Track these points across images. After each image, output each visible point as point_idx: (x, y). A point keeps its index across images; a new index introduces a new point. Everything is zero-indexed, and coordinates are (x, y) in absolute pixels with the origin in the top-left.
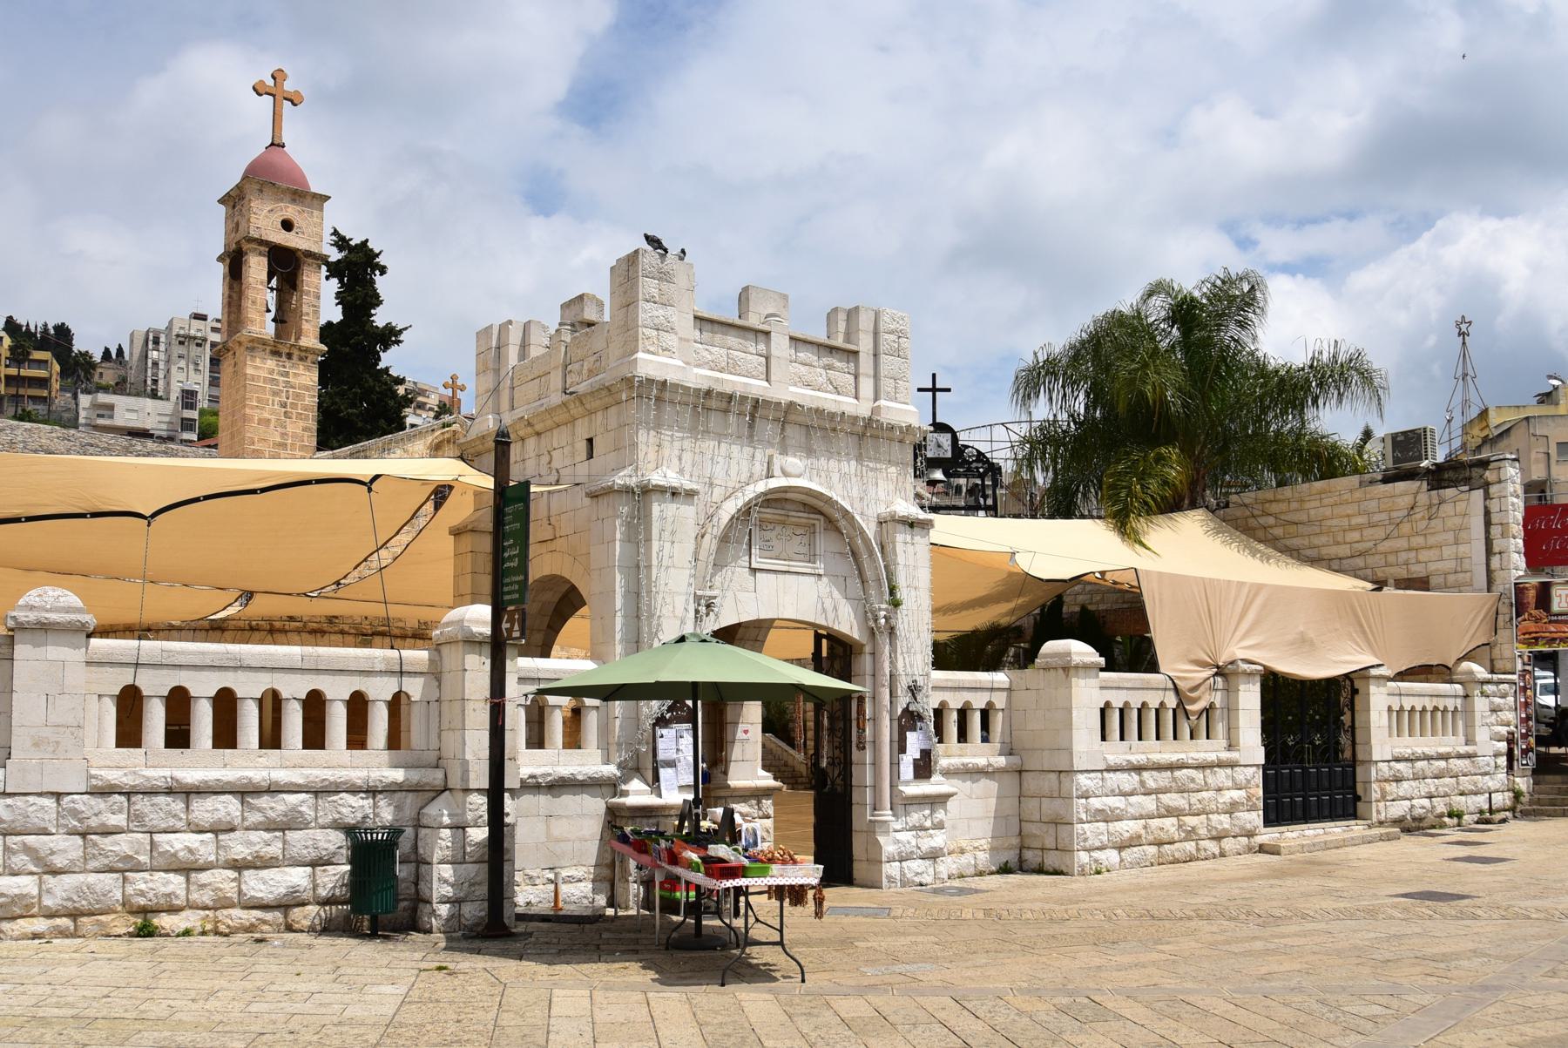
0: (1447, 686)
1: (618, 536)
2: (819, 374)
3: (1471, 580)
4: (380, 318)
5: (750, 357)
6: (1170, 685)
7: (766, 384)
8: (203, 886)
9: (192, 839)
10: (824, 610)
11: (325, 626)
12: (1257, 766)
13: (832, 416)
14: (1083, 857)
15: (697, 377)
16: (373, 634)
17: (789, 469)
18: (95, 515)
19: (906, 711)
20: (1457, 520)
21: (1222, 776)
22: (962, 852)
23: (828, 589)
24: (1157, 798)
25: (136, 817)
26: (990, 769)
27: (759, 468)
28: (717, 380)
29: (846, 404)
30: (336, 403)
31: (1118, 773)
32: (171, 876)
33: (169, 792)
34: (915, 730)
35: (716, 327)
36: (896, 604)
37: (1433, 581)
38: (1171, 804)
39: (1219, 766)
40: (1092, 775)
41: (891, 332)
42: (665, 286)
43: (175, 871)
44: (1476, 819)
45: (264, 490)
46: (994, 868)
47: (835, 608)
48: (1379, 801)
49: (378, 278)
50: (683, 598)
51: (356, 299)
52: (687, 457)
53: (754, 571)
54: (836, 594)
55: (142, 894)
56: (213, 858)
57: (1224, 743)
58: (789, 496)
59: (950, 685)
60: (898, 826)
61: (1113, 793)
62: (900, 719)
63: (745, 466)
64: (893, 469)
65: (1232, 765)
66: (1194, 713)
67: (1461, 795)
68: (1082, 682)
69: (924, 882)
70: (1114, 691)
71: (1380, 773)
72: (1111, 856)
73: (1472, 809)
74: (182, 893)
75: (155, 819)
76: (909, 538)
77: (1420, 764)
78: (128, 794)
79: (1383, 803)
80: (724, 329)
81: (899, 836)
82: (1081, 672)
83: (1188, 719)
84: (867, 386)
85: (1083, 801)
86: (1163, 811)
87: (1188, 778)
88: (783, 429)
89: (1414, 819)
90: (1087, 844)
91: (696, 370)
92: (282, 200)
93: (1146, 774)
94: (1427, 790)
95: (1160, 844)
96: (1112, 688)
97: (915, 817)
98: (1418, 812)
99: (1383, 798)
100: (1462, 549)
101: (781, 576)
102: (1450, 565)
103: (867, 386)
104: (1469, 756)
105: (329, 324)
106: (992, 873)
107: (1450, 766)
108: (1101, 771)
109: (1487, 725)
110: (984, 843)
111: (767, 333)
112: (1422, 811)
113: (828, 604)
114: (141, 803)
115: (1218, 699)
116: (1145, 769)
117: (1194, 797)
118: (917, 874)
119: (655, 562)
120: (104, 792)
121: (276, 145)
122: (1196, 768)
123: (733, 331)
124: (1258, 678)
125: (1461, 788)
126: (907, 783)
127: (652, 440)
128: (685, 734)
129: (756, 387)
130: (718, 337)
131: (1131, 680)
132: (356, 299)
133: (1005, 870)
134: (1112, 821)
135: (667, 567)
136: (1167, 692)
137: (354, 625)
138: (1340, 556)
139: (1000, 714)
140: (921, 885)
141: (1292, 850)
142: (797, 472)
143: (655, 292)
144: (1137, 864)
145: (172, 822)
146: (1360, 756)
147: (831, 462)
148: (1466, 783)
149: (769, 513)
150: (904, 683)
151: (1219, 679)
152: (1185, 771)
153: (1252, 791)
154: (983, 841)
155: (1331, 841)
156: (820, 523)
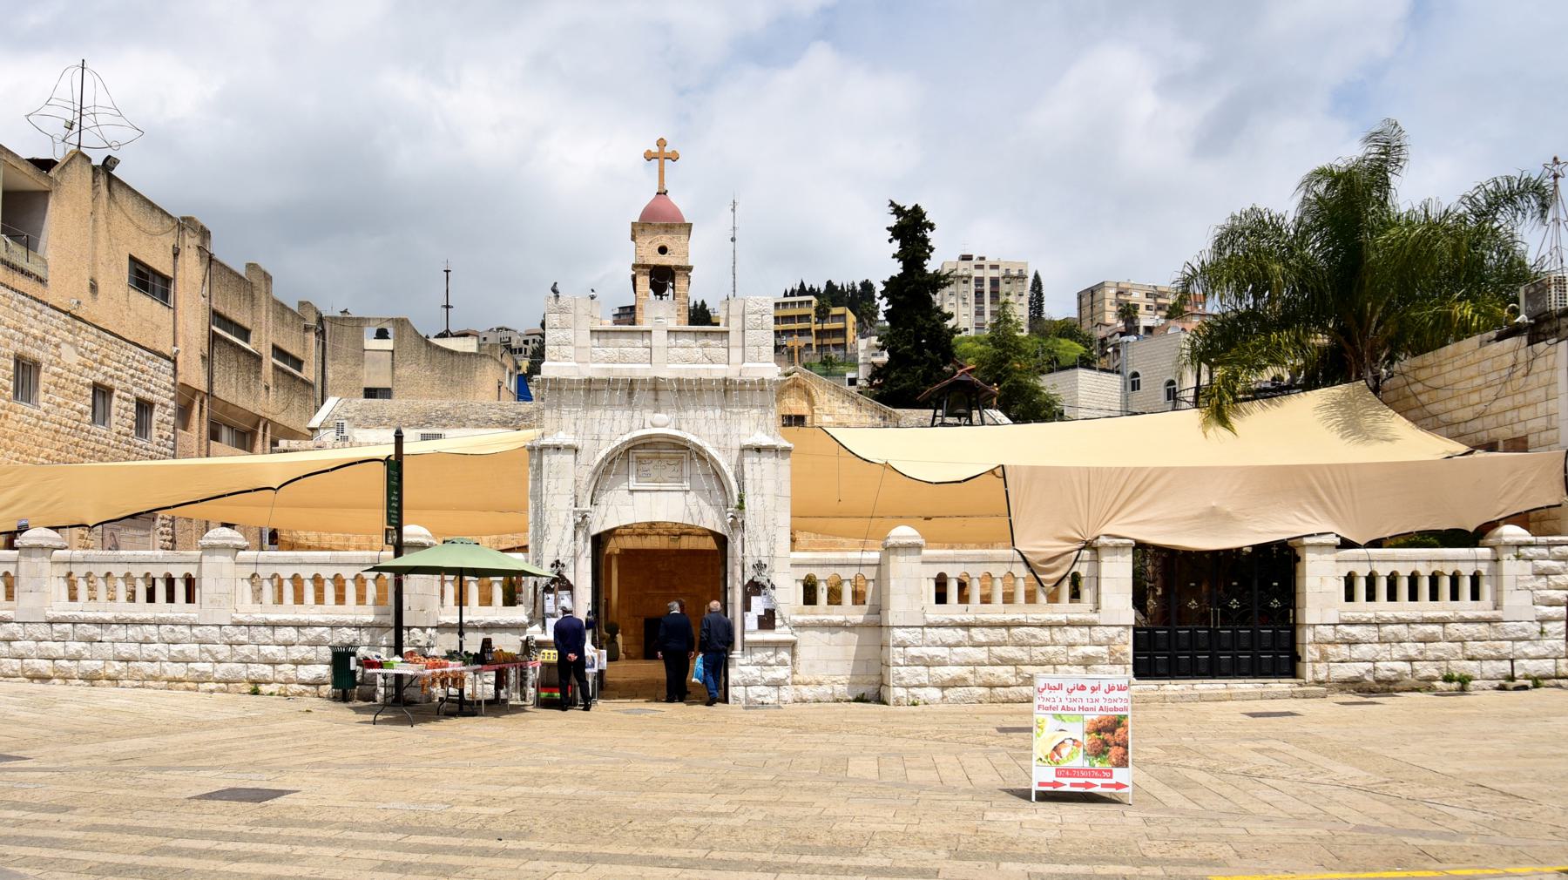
0: (1465, 550)
1: (530, 477)
2: (697, 352)
3: (1558, 437)
4: (931, 266)
5: (637, 350)
6: (1019, 558)
7: (649, 366)
8: (280, 672)
9: (274, 649)
10: (691, 514)
11: (647, 531)
12: (1127, 626)
13: (689, 382)
14: (899, 692)
15: (594, 370)
16: (681, 534)
17: (655, 422)
18: (256, 490)
19: (751, 582)
20: (1547, 375)
21: (1074, 634)
22: (820, 684)
23: (695, 500)
24: (989, 650)
25: (252, 637)
26: (848, 624)
27: (636, 423)
28: (608, 369)
29: (719, 371)
30: (893, 343)
31: (940, 629)
32: (266, 666)
33: (265, 625)
34: (759, 595)
35: (610, 335)
36: (741, 507)
37: (1532, 440)
38: (1003, 654)
39: (1068, 625)
40: (910, 629)
41: (755, 313)
42: (564, 317)
43: (269, 664)
44: (1497, 685)
45: (333, 469)
46: (850, 698)
47: (701, 512)
48: (1317, 662)
49: (929, 234)
50: (565, 513)
51: (907, 256)
52: (580, 423)
53: (632, 491)
54: (702, 502)
55: (253, 674)
56: (284, 658)
57: (1091, 606)
58: (653, 440)
59: (816, 562)
60: (744, 662)
61: (934, 644)
62: (747, 585)
63: (625, 423)
64: (755, 411)
65: (1090, 625)
66: (1048, 581)
67: (1469, 659)
68: (901, 559)
69: (765, 702)
70: (949, 565)
71: (1317, 635)
72: (935, 693)
73: (1491, 674)
74: (271, 675)
75: (260, 638)
76: (756, 460)
77: (1387, 629)
78: (248, 626)
79: (1324, 664)
80: (617, 334)
81: (743, 669)
82: (900, 551)
83: (1042, 585)
84: (736, 354)
85: (901, 649)
86: (994, 660)
87: (1027, 634)
88: (657, 394)
89: (1378, 681)
90: (903, 682)
91: (592, 366)
92: (657, 233)
93: (973, 631)
94: (1402, 653)
95: (991, 686)
96: (946, 562)
97: (759, 656)
98: (1381, 674)
99: (1324, 657)
100: (1551, 404)
101: (654, 494)
102: (1542, 423)
103: (736, 354)
104: (1489, 621)
105: (892, 278)
106: (849, 701)
107: (1447, 631)
108: (922, 627)
109: (1528, 589)
110: (843, 679)
111: (650, 332)
112: (1389, 674)
113: (694, 510)
114: (254, 630)
115: (1083, 569)
116: (975, 626)
117: (1036, 652)
118: (759, 696)
119: (544, 492)
120: (238, 624)
121: (662, 193)
122: (1042, 626)
123: (623, 335)
124: (1131, 550)
125: (1469, 653)
126: (752, 632)
127: (554, 416)
128: (565, 597)
129: (642, 371)
130: (611, 341)
131: (968, 555)
132: (907, 256)
133: (861, 699)
134: (933, 666)
135: (553, 495)
136: (1015, 565)
137: (667, 529)
138: (1466, 419)
139: (871, 584)
140: (763, 703)
141: (1148, 699)
142: (663, 423)
143: (556, 322)
144: (956, 702)
145: (266, 640)
146: (1299, 620)
147: (699, 412)
148: (1475, 648)
149: (642, 453)
150: (749, 562)
151: (1086, 554)
152: (1025, 629)
153: (1116, 648)
154: (841, 678)
155: (1210, 695)
156: (686, 457)
